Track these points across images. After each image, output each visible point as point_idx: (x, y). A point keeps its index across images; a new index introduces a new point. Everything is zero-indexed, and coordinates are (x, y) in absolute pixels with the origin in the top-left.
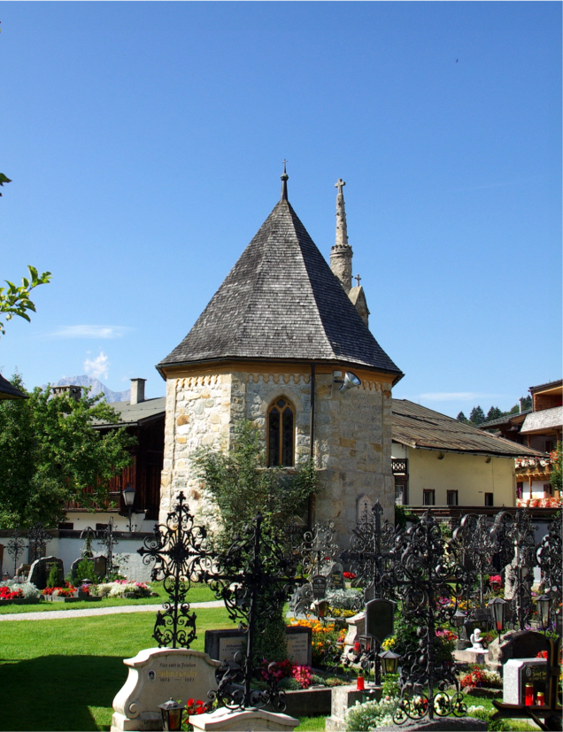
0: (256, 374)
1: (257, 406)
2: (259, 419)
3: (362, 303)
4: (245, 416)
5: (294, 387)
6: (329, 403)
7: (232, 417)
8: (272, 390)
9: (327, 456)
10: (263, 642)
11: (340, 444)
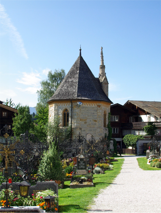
0: (60, 104)
1: (60, 112)
2: (60, 115)
3: (106, 81)
4: (57, 114)
5: (67, 106)
6: (76, 110)
7: (54, 115)
8: (63, 107)
9: (76, 124)
10: (116, 195)
11: (80, 121)
